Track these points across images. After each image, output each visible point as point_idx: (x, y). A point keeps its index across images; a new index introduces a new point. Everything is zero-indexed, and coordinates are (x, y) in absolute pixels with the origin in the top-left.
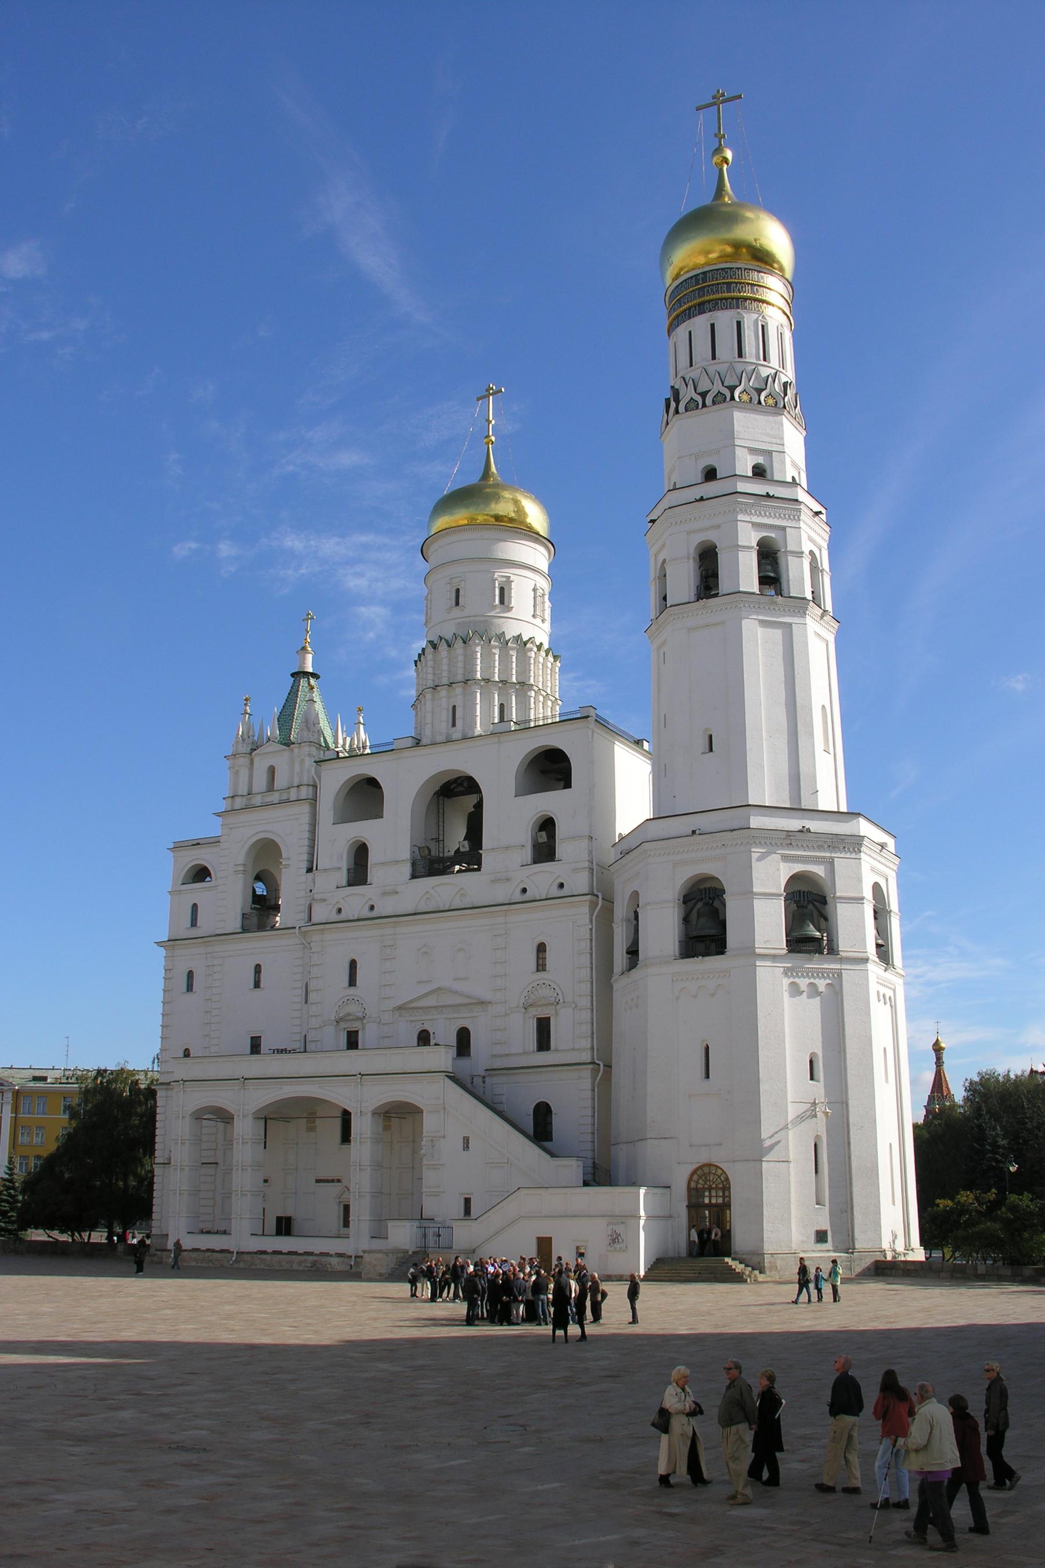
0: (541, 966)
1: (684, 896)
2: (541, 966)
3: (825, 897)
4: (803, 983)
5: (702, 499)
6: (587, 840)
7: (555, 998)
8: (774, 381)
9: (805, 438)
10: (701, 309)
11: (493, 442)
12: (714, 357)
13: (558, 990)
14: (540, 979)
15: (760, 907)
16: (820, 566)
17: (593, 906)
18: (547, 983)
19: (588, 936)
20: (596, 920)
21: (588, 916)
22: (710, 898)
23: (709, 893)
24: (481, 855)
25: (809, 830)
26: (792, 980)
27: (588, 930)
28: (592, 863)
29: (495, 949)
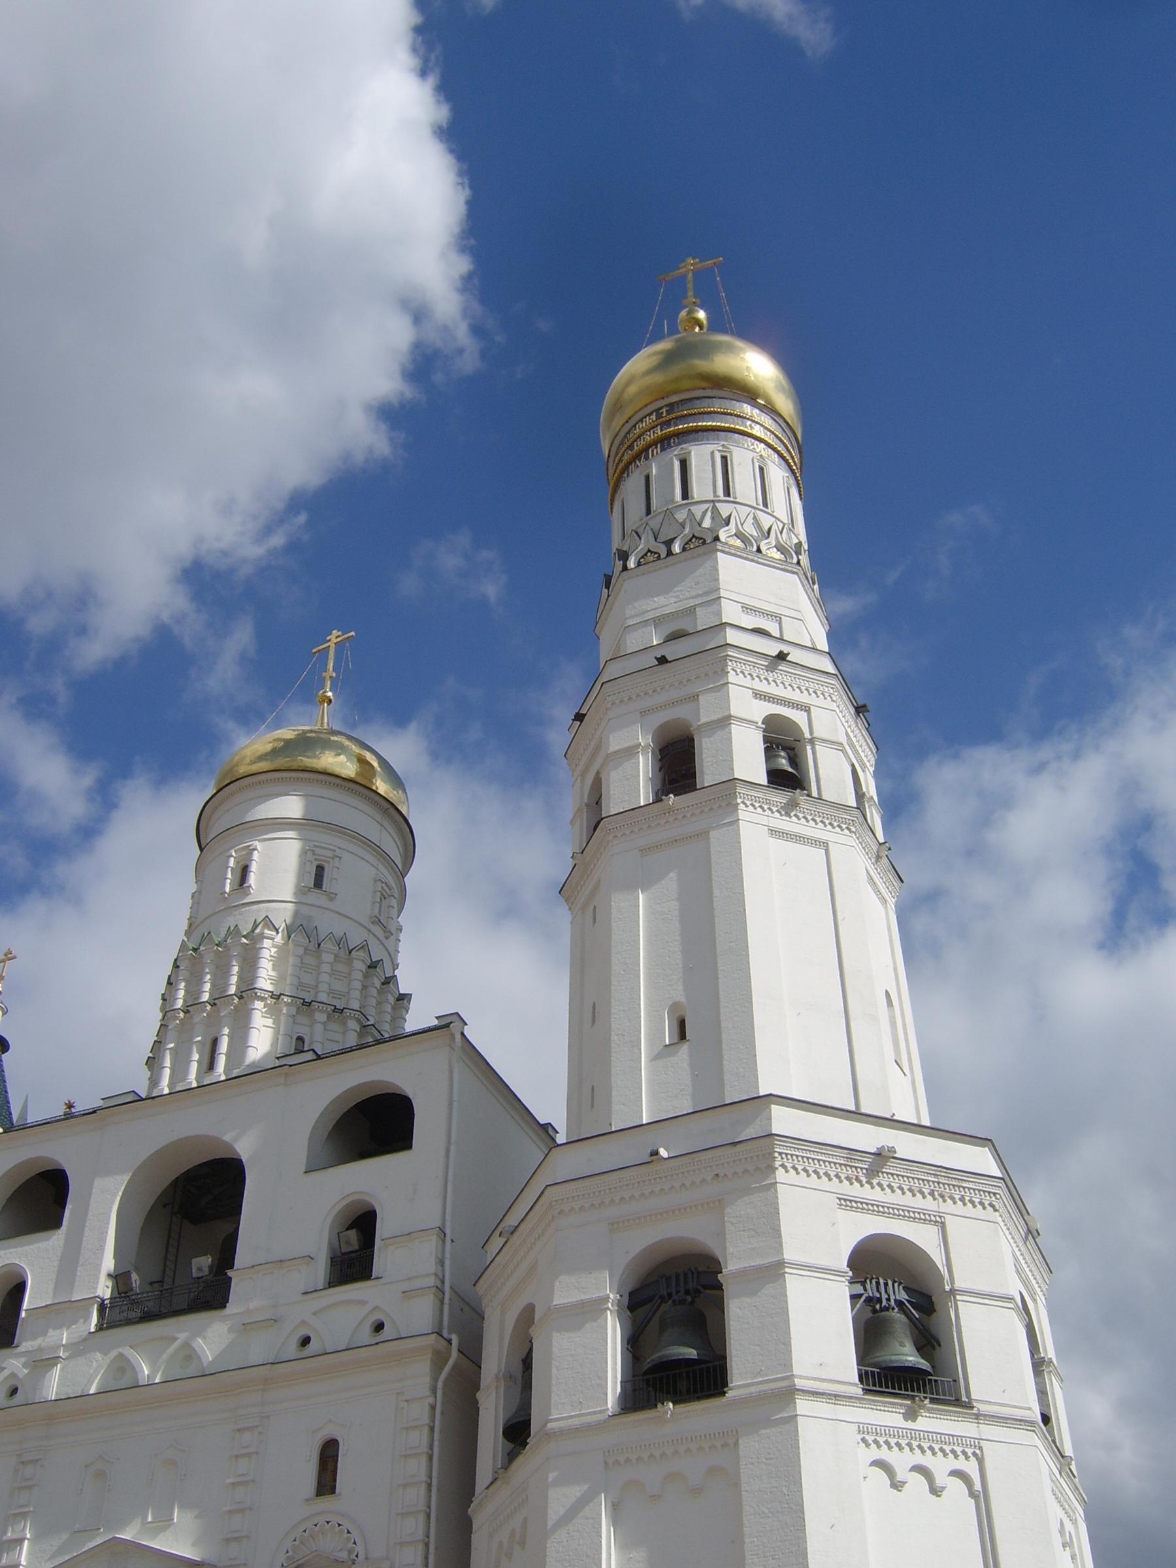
0: (326, 1483)
1: (631, 1294)
2: (326, 1483)
3: (931, 1297)
4: (901, 1461)
5: (662, 660)
6: (434, 1238)
7: (350, 1552)
8: (781, 533)
9: (827, 634)
10: (665, 442)
11: (330, 701)
12: (685, 494)
13: (355, 1534)
14: (318, 1514)
15: (796, 1287)
16: (864, 790)
17: (439, 1360)
18: (335, 1520)
19: (426, 1419)
20: (444, 1394)
21: (427, 1380)
22: (687, 1292)
23: (686, 1282)
24: (230, 1278)
25: (892, 1150)
26: (875, 1453)
27: (427, 1409)
28: (443, 1282)
29: (237, 1457)
